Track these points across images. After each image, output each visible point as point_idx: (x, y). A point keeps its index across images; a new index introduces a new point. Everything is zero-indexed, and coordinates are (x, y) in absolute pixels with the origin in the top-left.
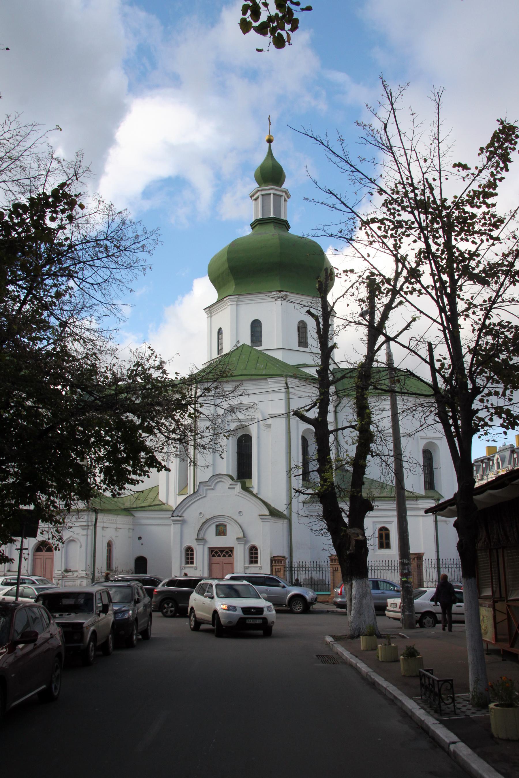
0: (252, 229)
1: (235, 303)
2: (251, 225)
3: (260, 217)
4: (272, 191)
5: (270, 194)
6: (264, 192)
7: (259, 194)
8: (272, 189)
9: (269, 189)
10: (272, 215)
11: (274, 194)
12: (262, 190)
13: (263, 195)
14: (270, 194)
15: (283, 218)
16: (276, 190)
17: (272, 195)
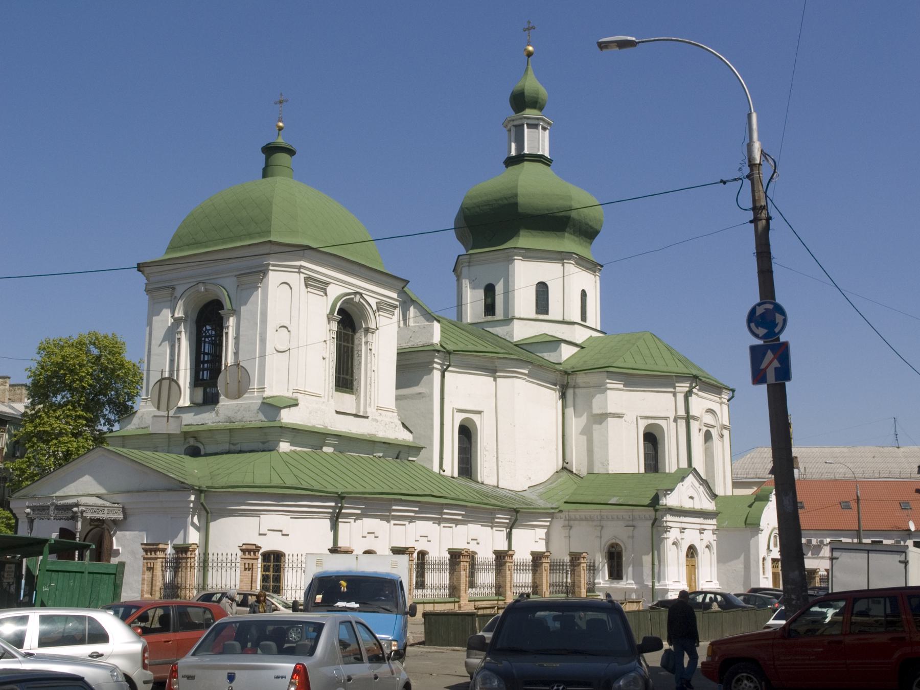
1: (467, 264)
4: (525, 122)
7: (513, 123)
11: (527, 124)
13: (515, 126)
14: (523, 125)
15: (540, 153)
17: (525, 126)
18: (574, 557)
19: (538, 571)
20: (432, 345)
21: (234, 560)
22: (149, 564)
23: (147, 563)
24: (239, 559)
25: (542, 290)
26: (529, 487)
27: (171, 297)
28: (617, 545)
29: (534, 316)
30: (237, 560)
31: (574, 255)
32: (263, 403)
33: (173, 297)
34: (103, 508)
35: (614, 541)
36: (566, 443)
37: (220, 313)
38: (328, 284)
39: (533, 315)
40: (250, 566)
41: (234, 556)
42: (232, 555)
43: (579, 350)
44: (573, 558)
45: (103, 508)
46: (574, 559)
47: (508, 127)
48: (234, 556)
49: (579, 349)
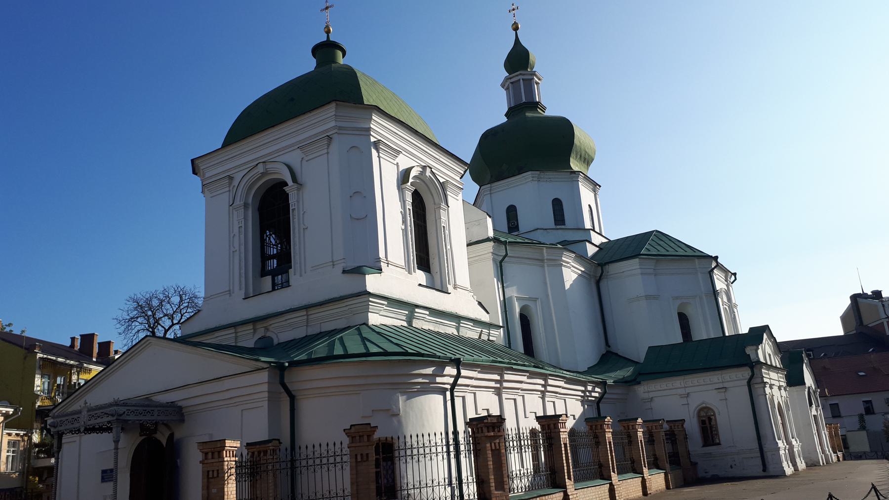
0: (507, 118)
1: (489, 192)
2: (506, 115)
3: (512, 105)
4: (521, 77)
5: (520, 80)
6: (512, 80)
7: (508, 83)
8: (521, 74)
9: (517, 75)
10: (524, 100)
11: (523, 79)
12: (511, 78)
13: (512, 83)
14: (520, 80)
16: (524, 75)
17: (521, 80)
18: (672, 425)
19: (656, 441)
20: (488, 238)
21: (339, 453)
22: (211, 473)
23: (208, 472)
24: (346, 450)
25: (557, 204)
26: (588, 368)
27: (229, 187)
28: (708, 409)
29: (554, 227)
30: (344, 452)
31: (581, 174)
32: (344, 272)
33: (232, 187)
34: (153, 409)
35: (704, 405)
36: (607, 325)
37: (284, 190)
38: (399, 152)
39: (554, 227)
40: (365, 458)
41: (338, 445)
42: (335, 444)
43: (598, 251)
44: (671, 427)
45: (153, 409)
46: (673, 427)
47: (506, 86)
48: (338, 445)
49: (598, 249)
